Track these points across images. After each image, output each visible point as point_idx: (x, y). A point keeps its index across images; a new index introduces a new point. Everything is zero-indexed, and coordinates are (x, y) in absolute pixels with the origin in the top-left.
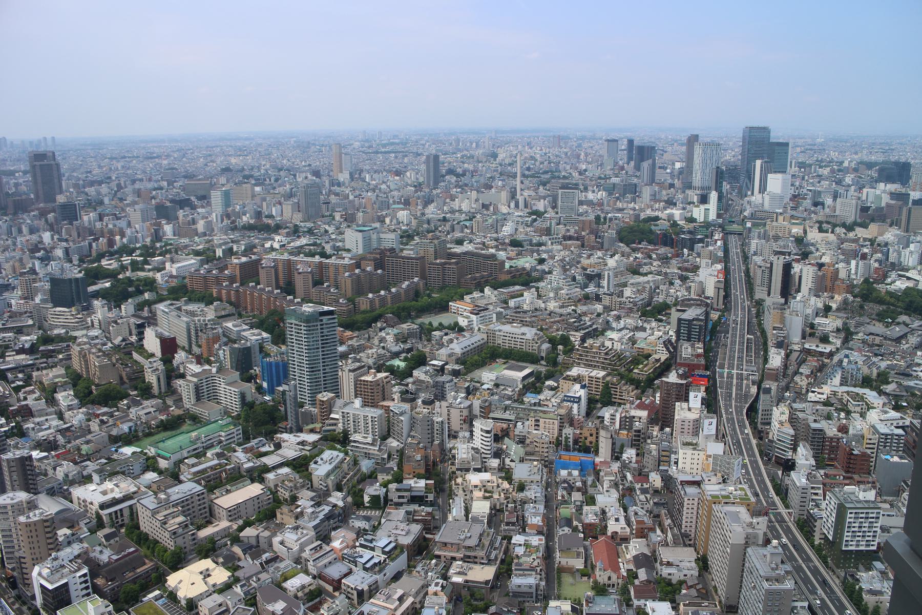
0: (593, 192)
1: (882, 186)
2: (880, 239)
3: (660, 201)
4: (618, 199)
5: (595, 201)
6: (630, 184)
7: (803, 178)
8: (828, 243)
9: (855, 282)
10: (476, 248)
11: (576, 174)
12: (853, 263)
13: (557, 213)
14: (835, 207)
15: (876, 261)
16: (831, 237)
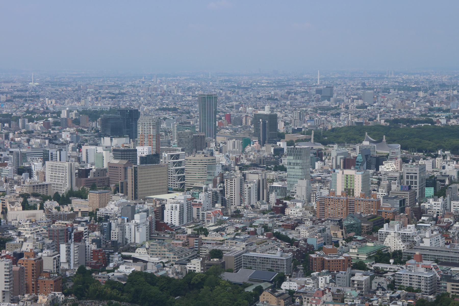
1: (106, 141)
2: (102, 211)
7: (7, 137)
8: (33, 223)
9: (68, 274)
12: (63, 247)
14: (44, 173)
15: (93, 241)
16: (40, 214)
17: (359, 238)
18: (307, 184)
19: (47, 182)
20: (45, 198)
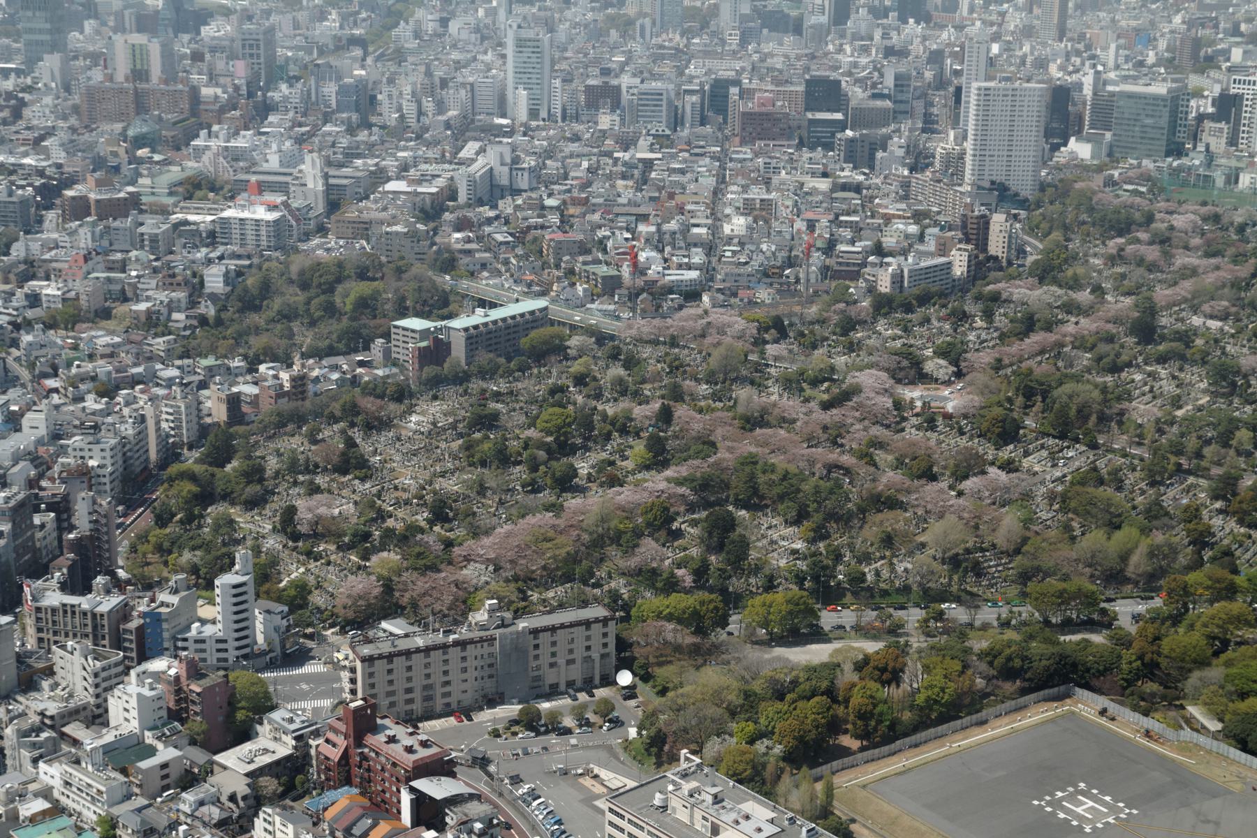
17: (157, 157)
18: (62, 62)
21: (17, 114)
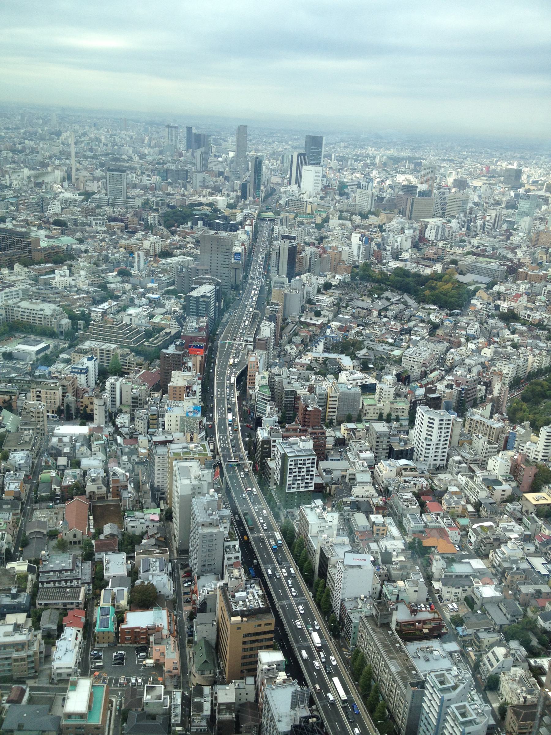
0: (148, 176)
3: (207, 188)
4: (169, 184)
5: (148, 185)
6: (182, 170)
10: (14, 226)
11: (136, 158)
13: (106, 195)
19: (357, 203)
20: (352, 214)
21: (508, 238)
